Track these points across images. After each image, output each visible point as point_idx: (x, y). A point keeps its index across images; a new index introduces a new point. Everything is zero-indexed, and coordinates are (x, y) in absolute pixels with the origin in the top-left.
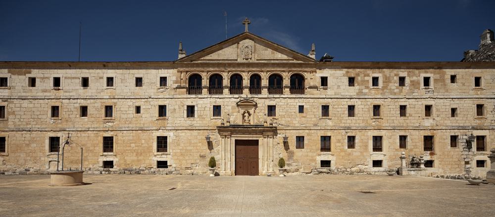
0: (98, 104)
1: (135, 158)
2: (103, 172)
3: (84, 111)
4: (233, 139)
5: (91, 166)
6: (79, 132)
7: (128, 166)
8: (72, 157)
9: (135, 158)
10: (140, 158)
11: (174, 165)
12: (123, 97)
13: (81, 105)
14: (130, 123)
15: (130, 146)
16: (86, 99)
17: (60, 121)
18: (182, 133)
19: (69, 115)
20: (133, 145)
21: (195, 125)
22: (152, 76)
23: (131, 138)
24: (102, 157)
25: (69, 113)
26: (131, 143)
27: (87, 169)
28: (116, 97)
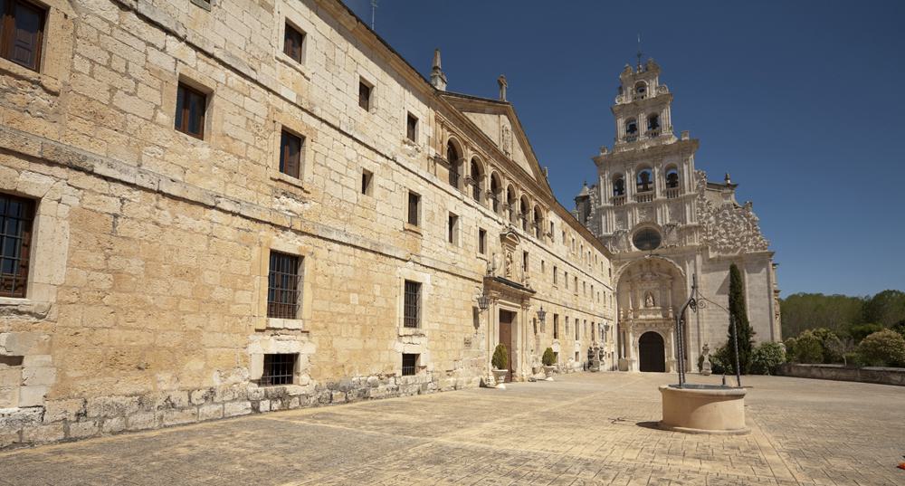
0: (257, 104)
1: (358, 344)
2: (264, 405)
3: (192, 105)
4: (498, 307)
5: (215, 380)
6: (164, 202)
7: (341, 373)
8: (117, 333)
9: (358, 344)
10: (371, 344)
11: (430, 367)
12: (337, 124)
13: (181, 69)
14: (349, 221)
15: (347, 302)
16: (210, 56)
17: (43, 100)
18: (443, 279)
19: (113, 90)
20: (354, 298)
21: (460, 265)
22: (395, 97)
23: (349, 272)
24: (260, 336)
25: (119, 82)
26: (350, 291)
27: (197, 395)
28: (318, 112)
